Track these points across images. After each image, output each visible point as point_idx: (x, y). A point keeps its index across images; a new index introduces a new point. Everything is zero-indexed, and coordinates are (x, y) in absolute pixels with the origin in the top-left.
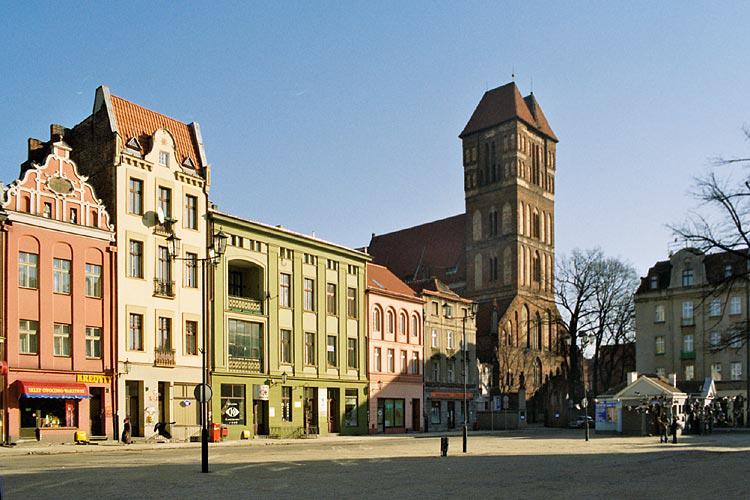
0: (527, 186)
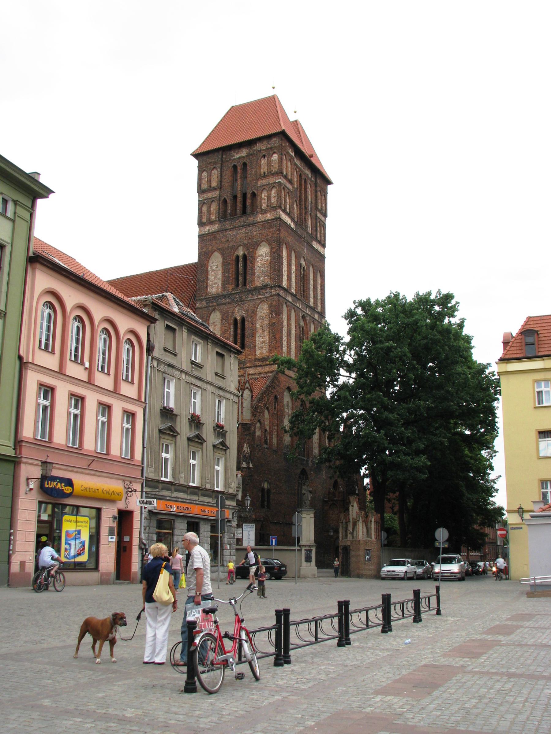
0: (292, 226)
